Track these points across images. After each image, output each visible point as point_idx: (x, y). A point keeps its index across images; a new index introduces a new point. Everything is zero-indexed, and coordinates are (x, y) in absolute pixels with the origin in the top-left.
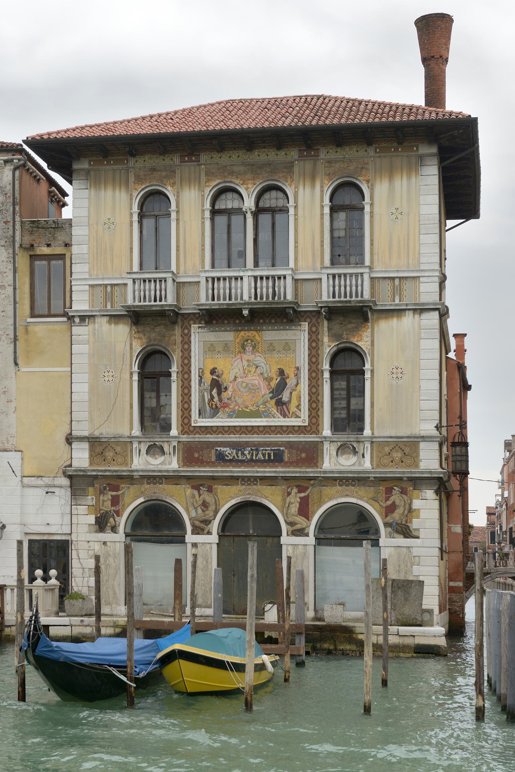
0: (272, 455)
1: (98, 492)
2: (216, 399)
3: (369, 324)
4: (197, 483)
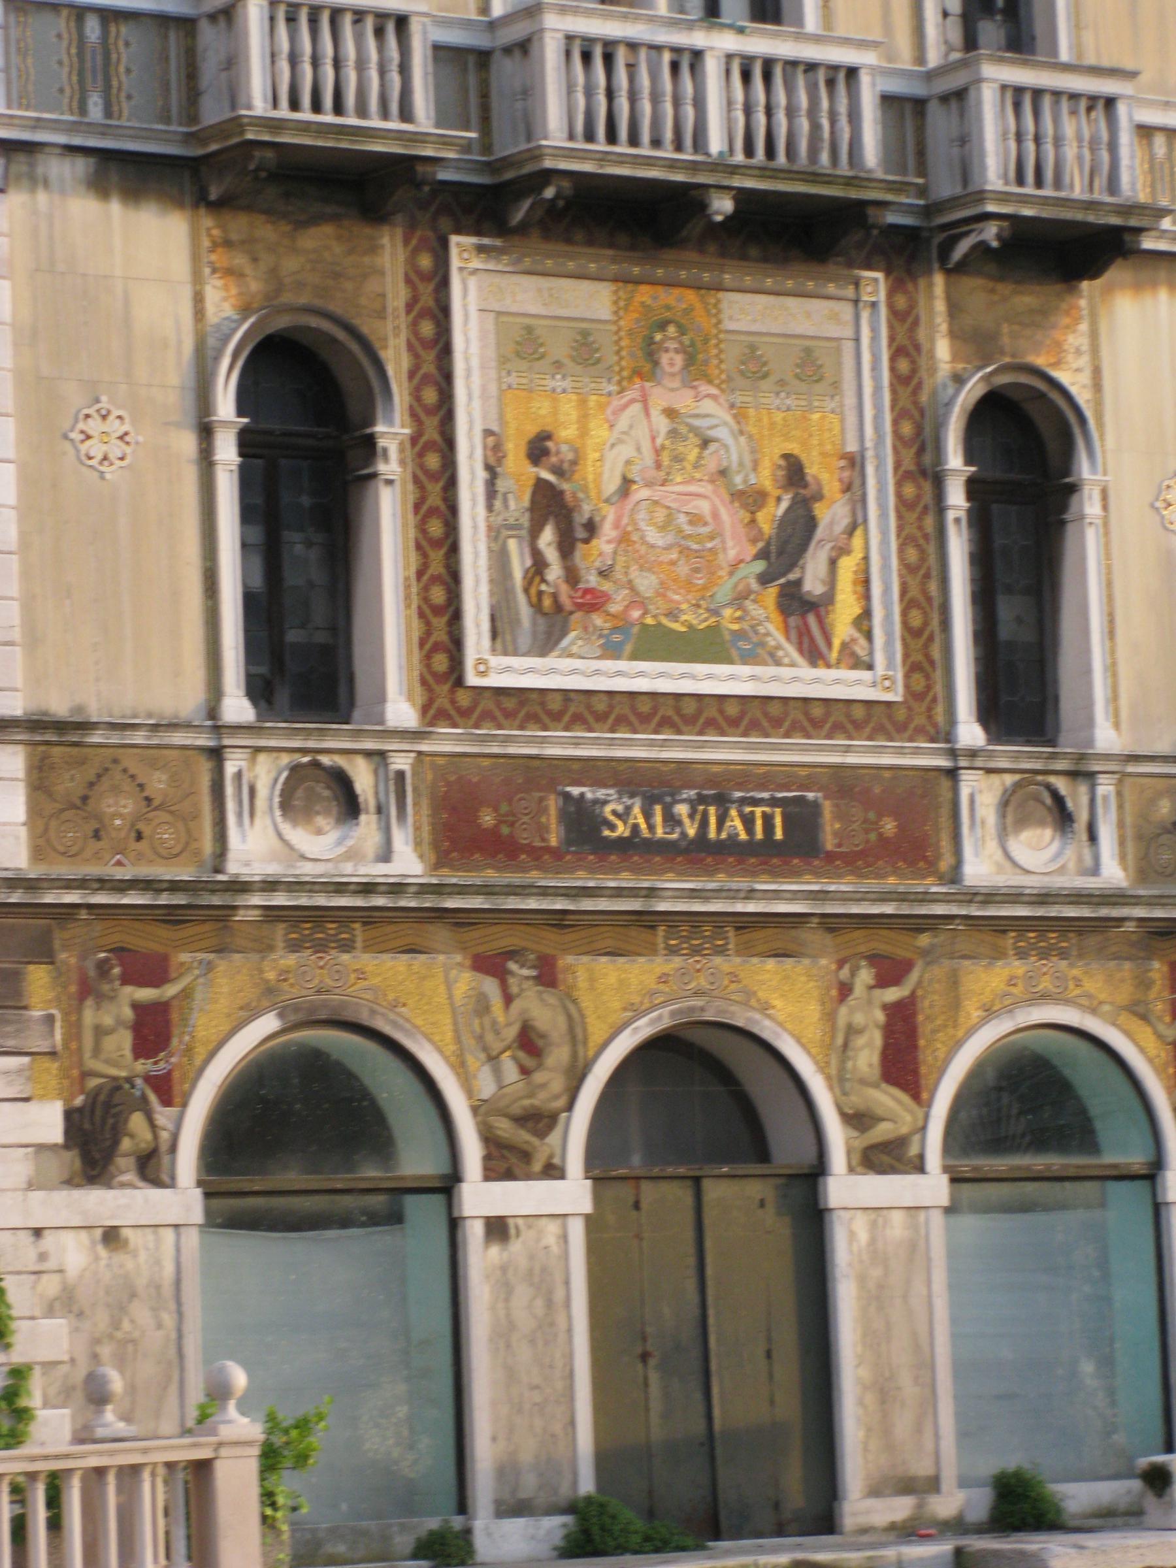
0: (778, 821)
1: (73, 989)
2: (555, 572)
3: (1083, 303)
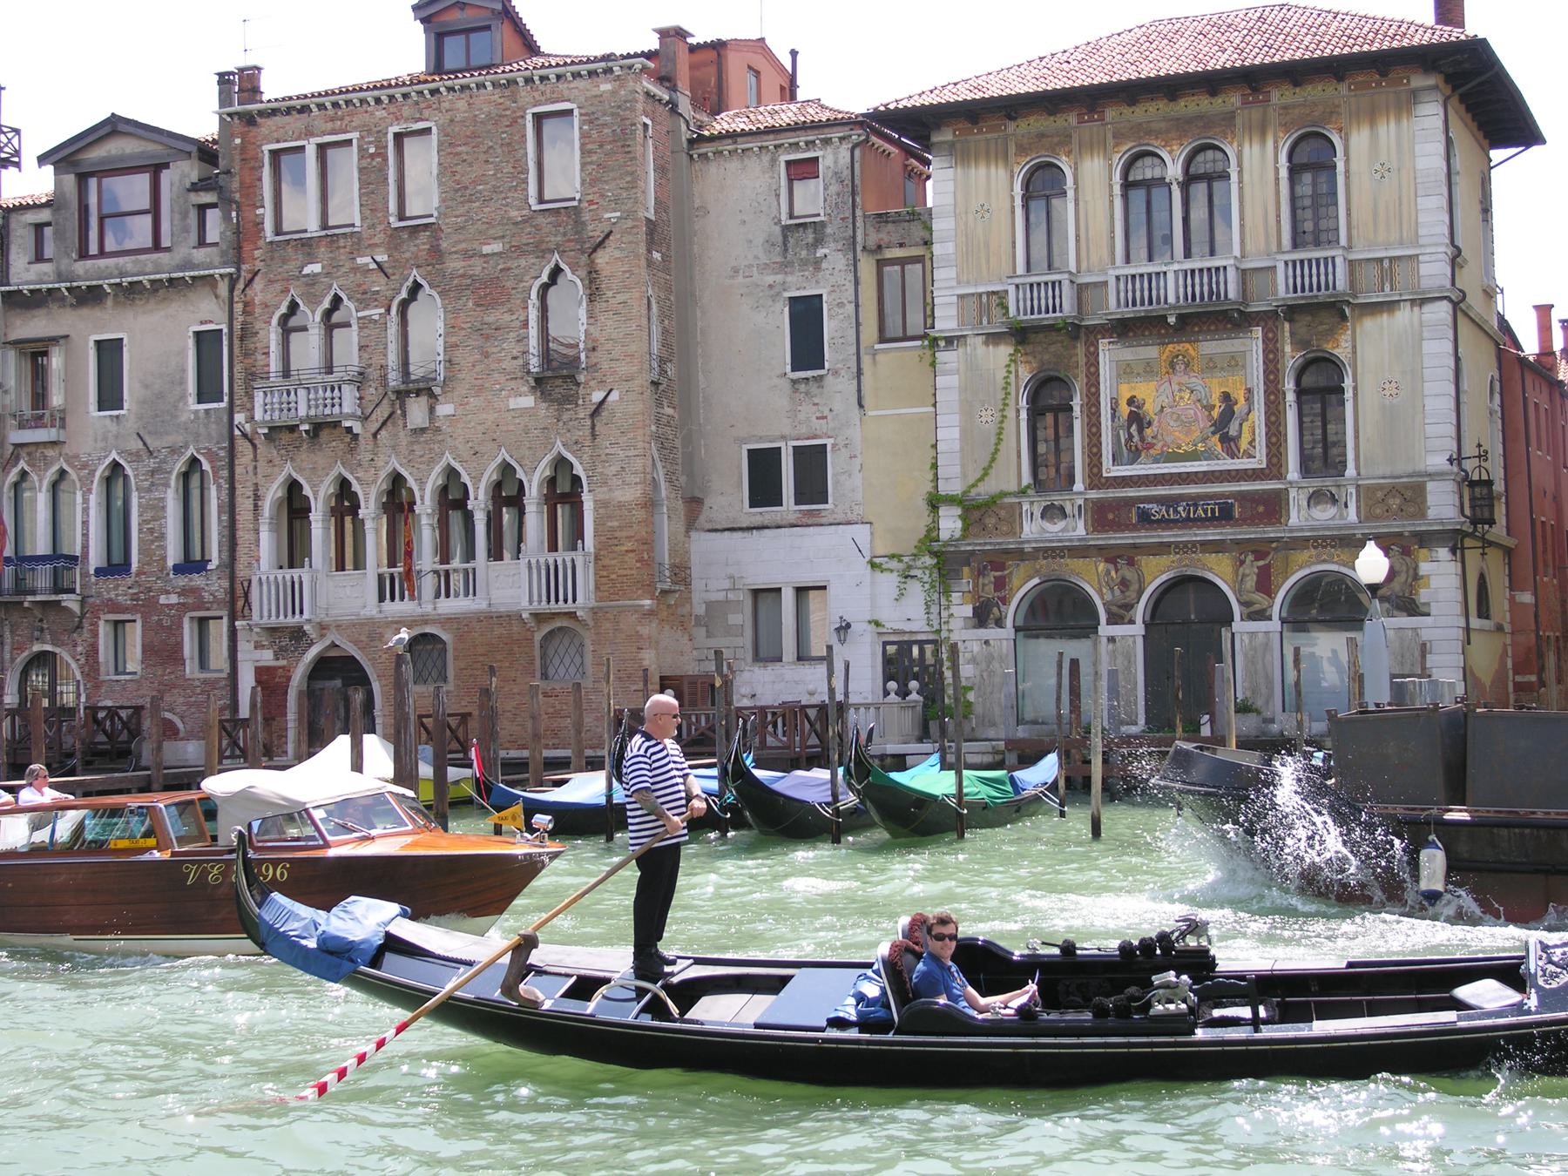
2: (1136, 438)
4: (1112, 555)
